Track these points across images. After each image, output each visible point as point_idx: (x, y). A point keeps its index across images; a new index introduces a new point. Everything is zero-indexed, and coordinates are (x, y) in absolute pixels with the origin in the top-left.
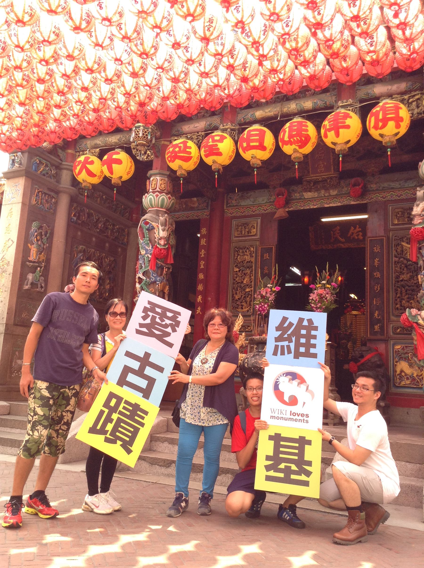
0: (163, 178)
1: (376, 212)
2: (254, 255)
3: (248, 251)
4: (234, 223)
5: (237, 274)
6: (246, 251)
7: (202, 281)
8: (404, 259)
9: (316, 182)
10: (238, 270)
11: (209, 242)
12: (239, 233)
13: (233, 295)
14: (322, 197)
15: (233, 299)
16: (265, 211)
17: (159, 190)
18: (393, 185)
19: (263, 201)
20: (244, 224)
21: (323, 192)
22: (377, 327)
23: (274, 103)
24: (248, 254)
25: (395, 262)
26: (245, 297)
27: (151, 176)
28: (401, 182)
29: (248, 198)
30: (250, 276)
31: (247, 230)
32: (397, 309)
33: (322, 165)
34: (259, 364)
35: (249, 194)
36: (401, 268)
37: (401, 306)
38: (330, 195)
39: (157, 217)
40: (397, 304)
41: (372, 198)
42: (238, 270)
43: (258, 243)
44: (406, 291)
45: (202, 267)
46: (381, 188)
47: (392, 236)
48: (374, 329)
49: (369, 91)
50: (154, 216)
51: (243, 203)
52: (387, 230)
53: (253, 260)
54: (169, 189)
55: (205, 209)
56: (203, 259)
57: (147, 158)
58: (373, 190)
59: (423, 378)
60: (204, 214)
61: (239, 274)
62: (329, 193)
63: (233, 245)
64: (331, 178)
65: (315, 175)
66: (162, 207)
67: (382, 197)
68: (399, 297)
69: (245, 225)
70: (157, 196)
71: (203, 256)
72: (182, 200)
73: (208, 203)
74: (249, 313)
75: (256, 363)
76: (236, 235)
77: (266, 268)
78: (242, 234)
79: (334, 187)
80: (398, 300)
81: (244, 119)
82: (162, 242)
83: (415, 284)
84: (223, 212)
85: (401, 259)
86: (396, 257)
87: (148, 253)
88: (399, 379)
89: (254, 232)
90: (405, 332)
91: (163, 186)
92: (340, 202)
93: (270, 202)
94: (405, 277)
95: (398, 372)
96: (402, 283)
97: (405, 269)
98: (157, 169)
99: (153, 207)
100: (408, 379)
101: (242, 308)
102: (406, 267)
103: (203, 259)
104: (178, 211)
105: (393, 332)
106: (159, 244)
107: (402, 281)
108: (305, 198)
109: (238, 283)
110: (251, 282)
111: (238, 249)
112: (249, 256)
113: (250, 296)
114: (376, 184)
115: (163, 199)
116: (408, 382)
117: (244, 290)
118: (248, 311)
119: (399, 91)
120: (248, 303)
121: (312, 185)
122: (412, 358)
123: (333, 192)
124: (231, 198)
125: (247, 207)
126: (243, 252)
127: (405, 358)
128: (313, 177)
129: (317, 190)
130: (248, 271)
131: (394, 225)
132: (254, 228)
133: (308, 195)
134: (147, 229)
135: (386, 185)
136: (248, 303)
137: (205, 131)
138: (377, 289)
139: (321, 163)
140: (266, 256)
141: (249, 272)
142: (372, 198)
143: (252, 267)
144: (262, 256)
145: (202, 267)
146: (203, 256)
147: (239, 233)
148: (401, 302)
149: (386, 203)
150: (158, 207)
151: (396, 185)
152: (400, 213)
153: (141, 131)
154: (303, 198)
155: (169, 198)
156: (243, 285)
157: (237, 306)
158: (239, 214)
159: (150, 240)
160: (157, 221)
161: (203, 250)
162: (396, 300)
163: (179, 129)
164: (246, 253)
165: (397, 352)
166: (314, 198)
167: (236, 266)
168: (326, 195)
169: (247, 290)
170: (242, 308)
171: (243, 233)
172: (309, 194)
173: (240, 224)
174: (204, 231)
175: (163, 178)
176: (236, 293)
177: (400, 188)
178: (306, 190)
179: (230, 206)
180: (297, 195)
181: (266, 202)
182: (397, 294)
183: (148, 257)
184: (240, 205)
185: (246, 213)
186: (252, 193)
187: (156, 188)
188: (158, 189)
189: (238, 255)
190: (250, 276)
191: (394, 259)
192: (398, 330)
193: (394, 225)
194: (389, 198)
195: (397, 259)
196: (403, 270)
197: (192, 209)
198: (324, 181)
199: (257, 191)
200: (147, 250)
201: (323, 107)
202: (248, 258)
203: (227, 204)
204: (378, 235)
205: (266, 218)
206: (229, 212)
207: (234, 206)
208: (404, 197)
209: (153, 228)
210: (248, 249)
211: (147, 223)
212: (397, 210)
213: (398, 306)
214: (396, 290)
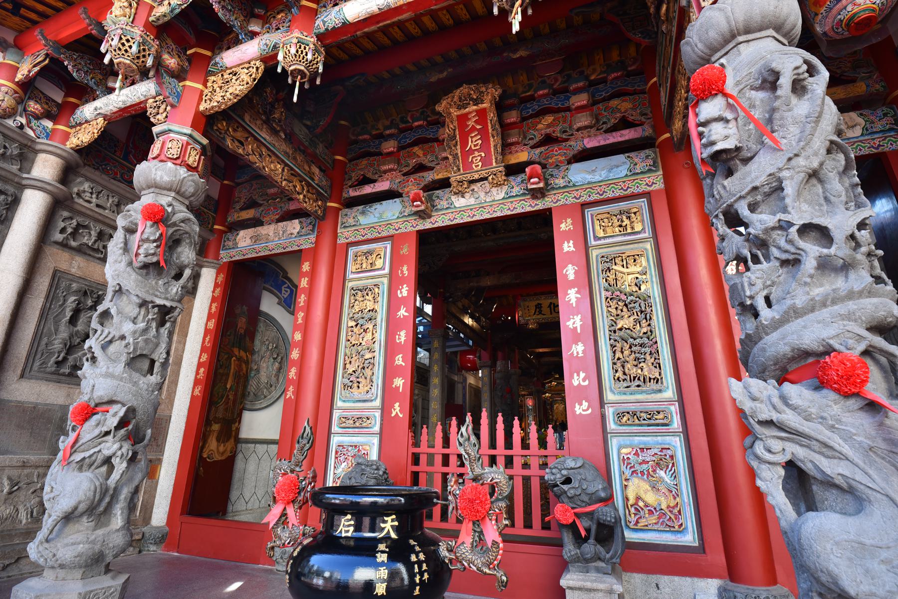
3: (370, 293)
10: (353, 324)
11: (312, 283)
24: (370, 297)
26: (363, 368)
33: (479, 158)
36: (616, 308)
37: (624, 374)
40: (617, 371)
42: (353, 324)
44: (630, 347)
55: (309, 234)
56: (301, 309)
59: (679, 512)
60: (307, 242)
61: (355, 329)
63: (350, 285)
68: (619, 359)
71: (302, 304)
80: (619, 364)
83: (644, 333)
88: (635, 514)
90: (637, 421)
94: (626, 322)
95: (632, 501)
96: (622, 333)
97: (625, 309)
100: (651, 512)
102: (626, 305)
107: (621, 329)
112: (372, 303)
116: (653, 519)
122: (654, 471)
127: (642, 473)
131: (597, 238)
133: (459, 202)
136: (368, 378)
141: (371, 327)
146: (302, 304)
147: (358, 266)
161: (303, 296)
167: (351, 318)
173: (360, 253)
174: (306, 267)
180: (444, 204)
181: (398, 218)
182: (614, 352)
192: (625, 419)
193: (597, 238)
195: (609, 294)
196: (622, 311)
199: (384, 202)
214: (613, 346)
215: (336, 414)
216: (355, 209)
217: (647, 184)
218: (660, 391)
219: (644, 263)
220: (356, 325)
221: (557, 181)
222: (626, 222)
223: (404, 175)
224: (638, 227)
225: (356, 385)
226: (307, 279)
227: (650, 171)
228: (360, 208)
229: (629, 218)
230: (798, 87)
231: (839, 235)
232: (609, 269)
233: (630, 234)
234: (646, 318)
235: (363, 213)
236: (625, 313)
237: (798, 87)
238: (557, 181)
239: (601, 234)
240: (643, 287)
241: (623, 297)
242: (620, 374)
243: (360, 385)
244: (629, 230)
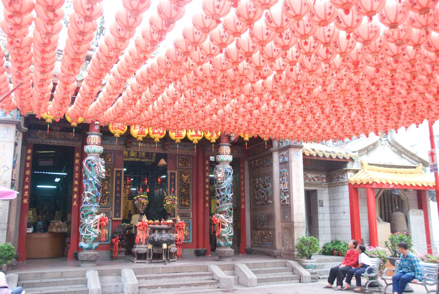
7: (76, 186)
21: (148, 144)
35: (107, 138)
45: (77, 177)
72: (61, 132)
73: (80, 138)
74: (107, 206)
77: (118, 181)
82: (104, 175)
103: (77, 172)
104: (59, 139)
145: (77, 177)
146: (77, 170)
169: (107, 193)
170: (103, 203)
193: (179, 166)
197: (69, 139)
208: (183, 154)
230: (230, 174)
231: (229, 198)
232: (181, 176)
236: (183, 188)
237: (230, 174)
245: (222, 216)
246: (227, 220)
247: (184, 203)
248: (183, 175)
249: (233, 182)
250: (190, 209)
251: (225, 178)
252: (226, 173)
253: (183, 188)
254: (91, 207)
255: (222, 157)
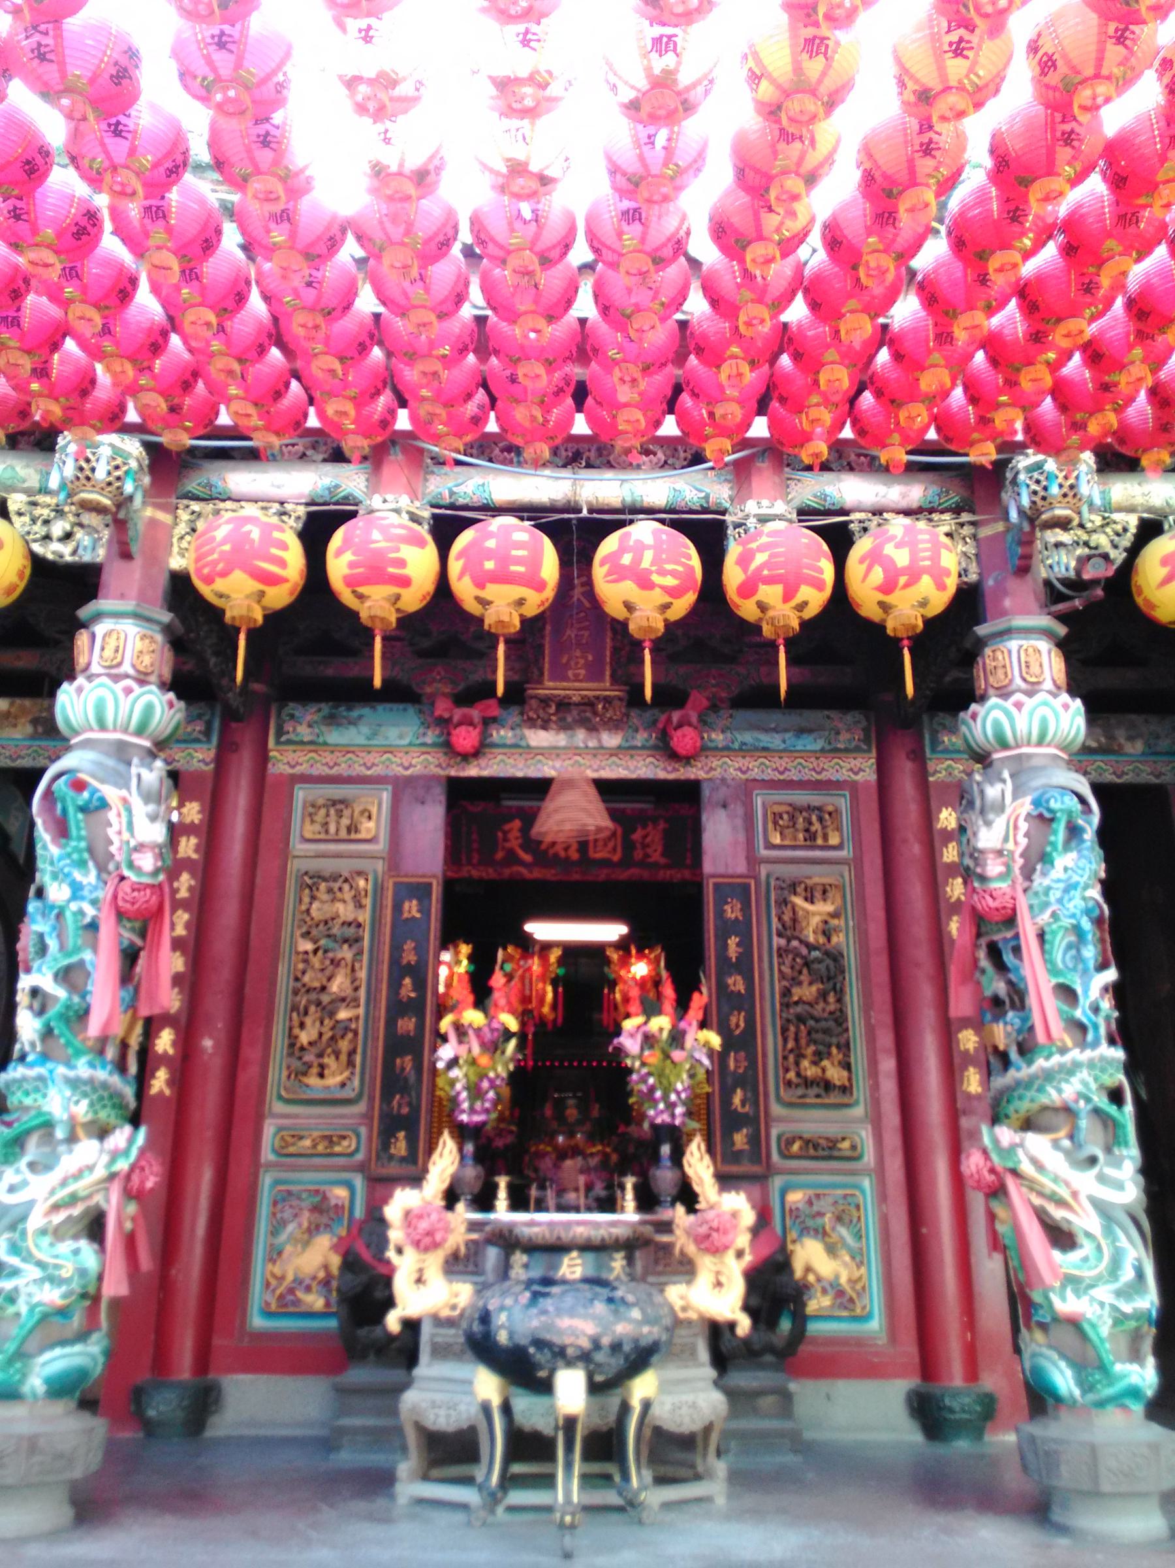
0: (149, 633)
1: (724, 806)
2: (368, 902)
4: (301, 794)
5: (306, 961)
6: (340, 889)
8: (801, 941)
9: (563, 705)
12: (317, 827)
13: (291, 1029)
14: (577, 748)
15: (292, 1045)
16: (407, 769)
17: (131, 672)
18: (766, 739)
19: (401, 737)
20: (334, 803)
22: (740, 1139)
23: (662, 467)
24: (348, 895)
25: (779, 949)
26: (333, 1038)
27: (98, 617)
28: (788, 735)
29: (353, 723)
30: (353, 970)
31: (345, 821)
32: (789, 1084)
33: (582, 661)
34: (560, 1332)
35: (355, 714)
36: (792, 968)
37: (798, 1074)
38: (602, 747)
39: (121, 767)
40: (787, 1070)
41: (711, 769)
42: (309, 946)
43: (380, 866)
44: (809, 1033)
46: (736, 746)
47: (768, 876)
48: (733, 1144)
49: (830, 490)
50: (111, 762)
51: (335, 736)
52: (753, 860)
53: (365, 917)
54: (167, 674)
57: (74, 553)
58: (716, 749)
59: (864, 1288)
61: (316, 961)
62: (599, 741)
64: (607, 700)
65: (558, 684)
66: (140, 732)
67: (740, 769)
68: (791, 1051)
69: (339, 805)
70: (128, 691)
74: (348, 1093)
75: (549, 1327)
76: (308, 835)
77: (409, 945)
78: (327, 832)
79: (614, 725)
80: (791, 1058)
81: (452, 493)
82: (147, 862)
83: (831, 1013)
84: (263, 758)
85: (795, 943)
86: (779, 935)
87: (83, 898)
89: (368, 830)
90: (812, 1152)
91: (147, 659)
92: (627, 768)
93: (424, 744)
94: (807, 991)
97: (805, 971)
98: (122, 596)
99: (103, 728)
100: (824, 1291)
101: (321, 1075)
102: (807, 964)
105: (780, 1152)
106: (131, 865)
107: (796, 1003)
108: (528, 747)
109: (308, 991)
110: (356, 989)
111: (312, 882)
112: (351, 906)
113: (350, 1035)
114: (723, 732)
115: (149, 708)
116: (826, 1301)
117: (332, 1014)
118: (343, 1085)
119: (904, 504)
120: (344, 1057)
121: (552, 710)
122: (833, 1229)
123: (611, 740)
124: (292, 716)
125: (348, 750)
126: (330, 891)
127: (816, 1231)
128: (550, 687)
129: (564, 727)
130: (346, 953)
131: (770, 846)
132: (370, 818)
133: (539, 738)
134: (83, 809)
135: (748, 737)
137: (307, 504)
138: (737, 1026)
139: (578, 653)
140: (412, 908)
142: (711, 769)
143: (358, 940)
144: (397, 908)
148: (797, 1064)
149: (748, 788)
150: (125, 730)
151: (774, 741)
152: (785, 816)
153: (103, 461)
154: (523, 743)
155: (171, 705)
156: (325, 999)
157: (304, 1068)
158: (320, 770)
159: (90, 850)
160: (122, 781)
162: (785, 1058)
163: (214, 480)
164: (339, 895)
165: (795, 1213)
166: (556, 748)
168: (591, 744)
169: (343, 1015)
170: (321, 1075)
171: (332, 828)
172: (542, 734)
173: (321, 802)
175: (149, 633)
176: (302, 1026)
177: (785, 750)
178: (532, 723)
179: (289, 742)
181: (410, 744)
182: (785, 1040)
183: (81, 913)
184: (325, 744)
185: (342, 770)
186: (366, 711)
187: (120, 664)
188: (127, 668)
189: (313, 898)
190: (353, 970)
191: (778, 942)
193: (770, 846)
194: (755, 773)
195: (783, 942)
196: (800, 972)
198: (589, 704)
199: (380, 708)
200: (77, 890)
201: (696, 507)
202: (345, 911)
203: (280, 732)
204: (730, 871)
205: (404, 789)
206: (282, 761)
207: (302, 743)
208: (794, 775)
209: (104, 805)
210: (346, 880)
211: (79, 786)
212: (777, 809)
213: (791, 1075)
214: (784, 1030)
215: (269, 1130)
216: (313, 708)
217: (851, 770)
218: (847, 1106)
219: (839, 901)
220: (315, 951)
221: (713, 736)
222: (816, 826)
223: (422, 654)
224: (834, 840)
225: (315, 1070)
226: (193, 841)
227: (857, 749)
228: (326, 708)
229: (821, 819)
232: (785, 902)
233: (822, 848)
234: (834, 989)
235: (332, 720)
236: (805, 977)
238: (713, 736)
239: (777, 840)
240: (834, 940)
241: (804, 951)
242: (791, 1075)
243: (326, 1072)
244: (820, 842)
245: (1036, 1143)
246: (1086, 1182)
247: (811, 1071)
248: (798, 901)
249: (1109, 887)
250: (859, 1111)
251: (1037, 859)
252: (1043, 819)
253: (805, 977)
254: (41, 1078)
255: (997, 714)
